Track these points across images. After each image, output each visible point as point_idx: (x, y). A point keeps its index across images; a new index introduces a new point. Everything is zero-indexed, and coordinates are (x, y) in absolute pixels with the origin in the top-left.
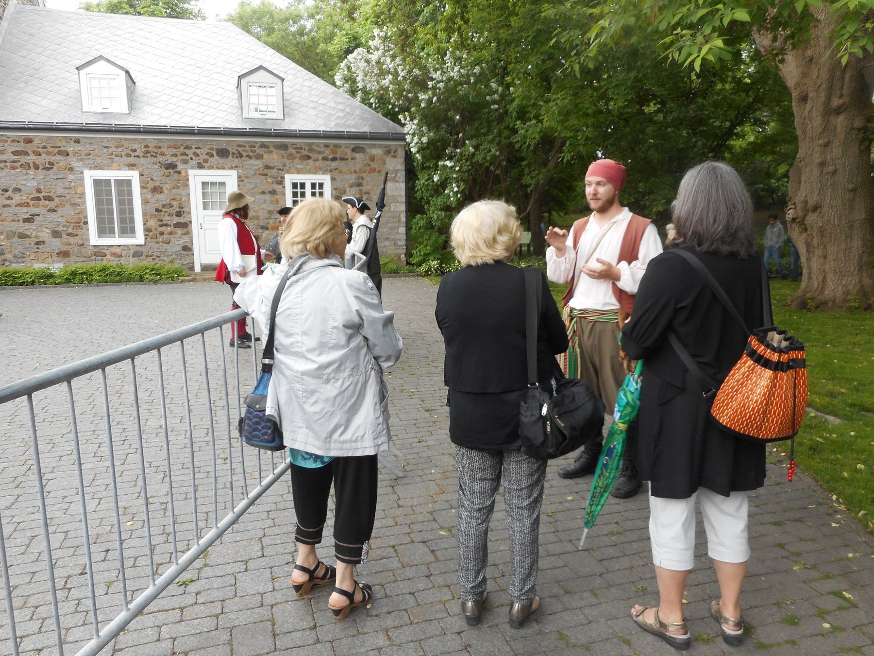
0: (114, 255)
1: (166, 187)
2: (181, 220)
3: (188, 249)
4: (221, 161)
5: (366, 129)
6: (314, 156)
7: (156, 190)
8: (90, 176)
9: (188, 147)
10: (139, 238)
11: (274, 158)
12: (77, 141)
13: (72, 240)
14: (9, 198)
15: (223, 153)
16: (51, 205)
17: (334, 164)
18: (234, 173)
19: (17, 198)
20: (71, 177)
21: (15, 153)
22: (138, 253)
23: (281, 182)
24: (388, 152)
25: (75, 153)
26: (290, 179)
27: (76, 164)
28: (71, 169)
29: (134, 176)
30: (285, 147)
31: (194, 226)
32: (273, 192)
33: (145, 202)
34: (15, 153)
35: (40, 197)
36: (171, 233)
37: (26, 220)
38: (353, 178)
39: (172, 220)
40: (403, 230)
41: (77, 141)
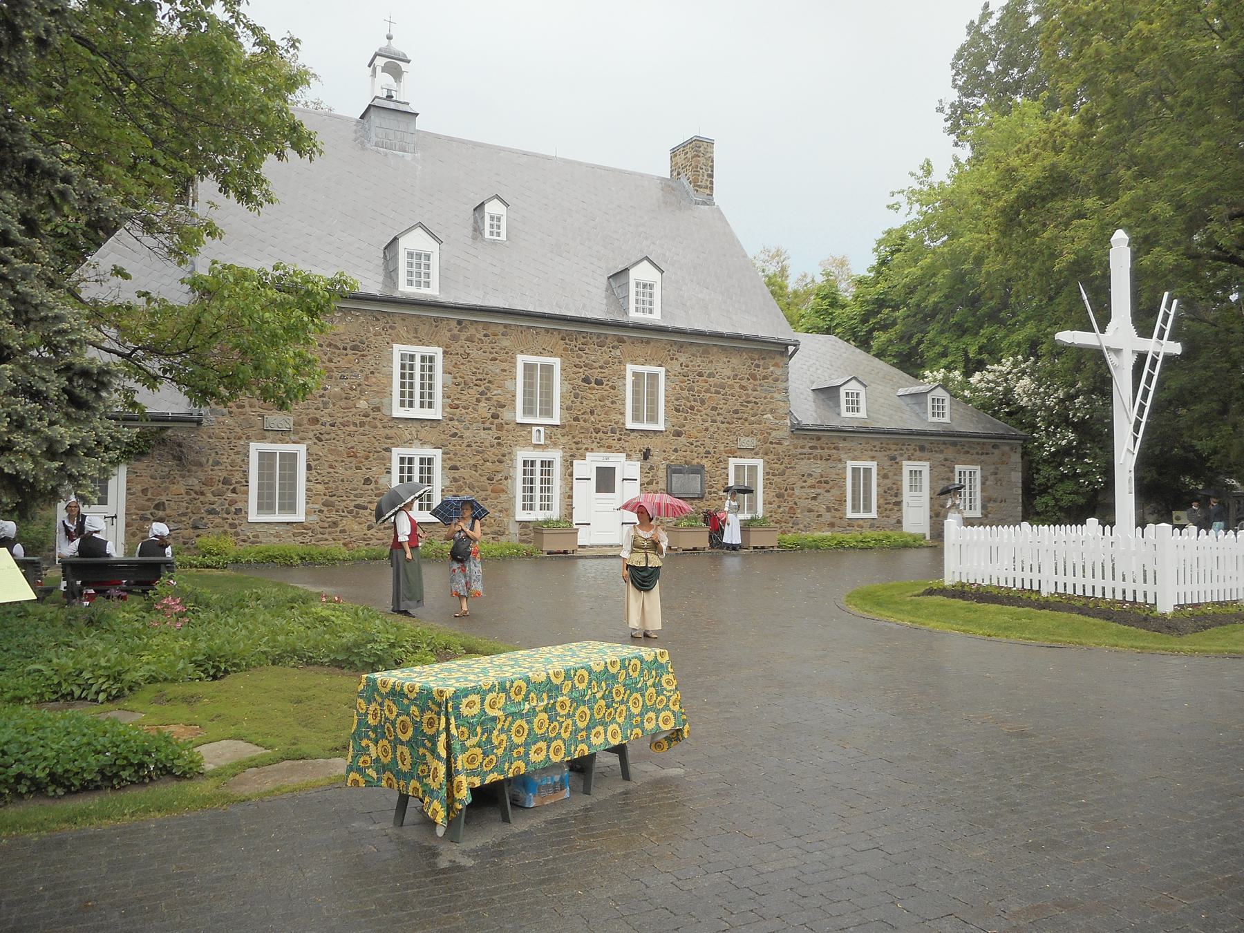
1: (890, 474)
3: (899, 522)
5: (980, 430)
7: (885, 477)
8: (851, 464)
10: (874, 515)
11: (950, 453)
13: (838, 514)
15: (922, 449)
16: (828, 487)
17: (983, 457)
18: (927, 464)
21: (811, 448)
22: (872, 524)
23: (952, 471)
24: (1012, 449)
25: (843, 448)
26: (958, 468)
27: (843, 456)
29: (873, 465)
31: (904, 504)
34: (811, 448)
35: (823, 481)
37: (814, 499)
38: (992, 469)
39: (892, 500)
40: (1020, 509)
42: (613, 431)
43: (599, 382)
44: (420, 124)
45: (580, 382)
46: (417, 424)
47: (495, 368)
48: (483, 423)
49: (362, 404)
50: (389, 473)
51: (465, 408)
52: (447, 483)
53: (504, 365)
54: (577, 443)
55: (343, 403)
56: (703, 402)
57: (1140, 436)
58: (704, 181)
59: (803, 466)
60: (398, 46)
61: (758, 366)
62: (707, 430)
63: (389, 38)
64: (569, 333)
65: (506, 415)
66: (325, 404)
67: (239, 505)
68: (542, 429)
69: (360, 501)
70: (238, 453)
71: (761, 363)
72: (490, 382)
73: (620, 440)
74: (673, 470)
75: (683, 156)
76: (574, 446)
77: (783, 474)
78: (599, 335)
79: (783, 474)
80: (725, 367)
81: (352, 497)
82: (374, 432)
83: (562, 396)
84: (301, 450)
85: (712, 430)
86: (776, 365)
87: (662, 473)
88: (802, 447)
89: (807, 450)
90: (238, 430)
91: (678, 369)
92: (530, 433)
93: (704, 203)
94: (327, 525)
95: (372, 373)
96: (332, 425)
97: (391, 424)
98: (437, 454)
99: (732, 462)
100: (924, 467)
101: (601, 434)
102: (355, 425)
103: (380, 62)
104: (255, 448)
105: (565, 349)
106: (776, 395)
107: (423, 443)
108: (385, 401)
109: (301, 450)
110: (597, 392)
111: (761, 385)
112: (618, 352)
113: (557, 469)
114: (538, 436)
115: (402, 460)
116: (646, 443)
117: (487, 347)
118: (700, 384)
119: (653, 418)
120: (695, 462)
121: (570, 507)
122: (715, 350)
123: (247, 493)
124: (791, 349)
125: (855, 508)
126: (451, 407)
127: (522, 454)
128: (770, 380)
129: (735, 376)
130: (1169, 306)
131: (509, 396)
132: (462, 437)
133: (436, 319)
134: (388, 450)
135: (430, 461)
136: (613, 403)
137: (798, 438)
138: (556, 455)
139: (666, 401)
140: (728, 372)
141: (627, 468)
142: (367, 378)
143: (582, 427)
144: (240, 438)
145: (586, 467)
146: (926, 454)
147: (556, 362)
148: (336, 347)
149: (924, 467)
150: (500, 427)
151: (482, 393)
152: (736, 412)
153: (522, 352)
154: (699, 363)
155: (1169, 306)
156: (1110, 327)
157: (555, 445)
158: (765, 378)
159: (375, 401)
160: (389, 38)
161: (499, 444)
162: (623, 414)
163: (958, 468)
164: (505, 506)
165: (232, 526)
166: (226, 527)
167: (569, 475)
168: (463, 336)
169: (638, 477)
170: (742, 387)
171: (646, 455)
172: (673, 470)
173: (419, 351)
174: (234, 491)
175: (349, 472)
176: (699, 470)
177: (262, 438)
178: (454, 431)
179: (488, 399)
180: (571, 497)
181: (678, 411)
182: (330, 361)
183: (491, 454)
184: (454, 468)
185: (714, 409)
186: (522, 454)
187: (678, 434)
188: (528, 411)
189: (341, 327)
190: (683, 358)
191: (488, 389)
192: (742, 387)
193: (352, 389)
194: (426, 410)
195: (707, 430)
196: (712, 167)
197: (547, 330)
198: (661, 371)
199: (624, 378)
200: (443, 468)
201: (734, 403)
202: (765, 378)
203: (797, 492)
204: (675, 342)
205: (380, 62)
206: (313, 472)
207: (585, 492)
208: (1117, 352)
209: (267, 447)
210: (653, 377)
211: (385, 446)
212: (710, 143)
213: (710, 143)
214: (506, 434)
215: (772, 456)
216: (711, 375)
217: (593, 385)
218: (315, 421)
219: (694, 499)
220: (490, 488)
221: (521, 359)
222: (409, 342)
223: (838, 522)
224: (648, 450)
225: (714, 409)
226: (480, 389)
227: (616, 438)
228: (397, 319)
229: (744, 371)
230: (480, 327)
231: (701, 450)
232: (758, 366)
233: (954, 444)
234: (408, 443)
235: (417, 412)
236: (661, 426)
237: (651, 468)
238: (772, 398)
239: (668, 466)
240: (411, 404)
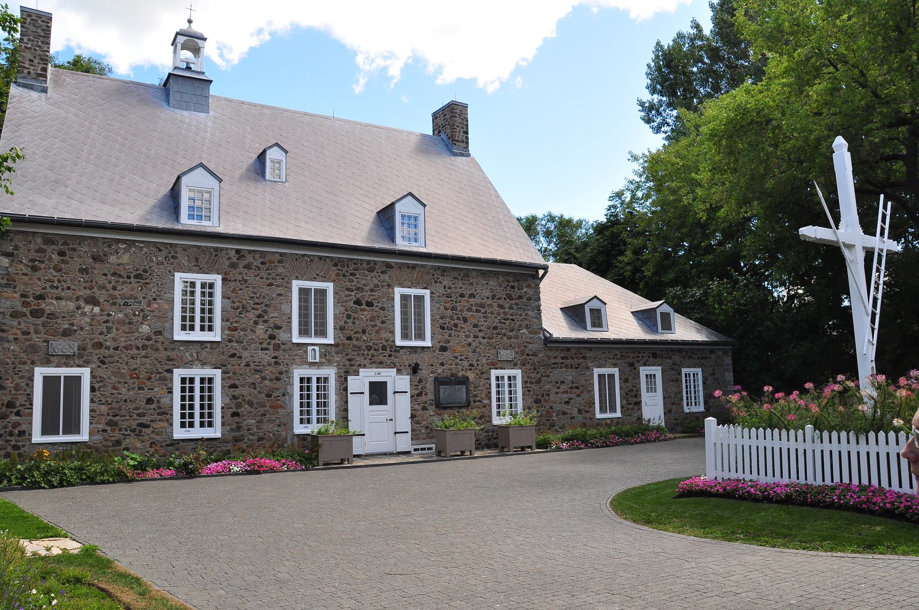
0: (607, 424)
1: (630, 378)
2: (637, 400)
4: (655, 360)
6: (694, 356)
8: (597, 371)
9: (640, 353)
10: (618, 414)
11: (677, 358)
12: (591, 349)
13: (588, 415)
14: (559, 388)
15: (655, 356)
19: (563, 388)
20: (588, 373)
21: (562, 358)
23: (680, 374)
24: (724, 353)
26: (684, 371)
27: (590, 365)
28: (588, 368)
29: (615, 371)
30: (680, 351)
31: (643, 404)
32: (677, 380)
33: (621, 389)
34: (562, 358)
36: (633, 409)
37: (567, 403)
39: (633, 400)
41: (591, 349)
42: (384, 348)
43: (369, 304)
44: (213, 90)
45: (352, 304)
46: (198, 347)
47: (273, 292)
48: (261, 343)
50: (171, 392)
51: (243, 330)
52: (227, 401)
53: (280, 290)
54: (350, 360)
55: (126, 328)
56: (465, 320)
57: (877, 326)
58: (460, 136)
59: (556, 375)
60: (196, 28)
61: (513, 287)
62: (470, 345)
63: (190, 22)
64: (341, 260)
65: (282, 336)
66: (109, 330)
67: (23, 427)
68: (317, 348)
69: (144, 420)
70: (22, 377)
71: (516, 284)
72: (266, 305)
73: (390, 356)
74: (439, 382)
75: (442, 118)
76: (347, 363)
77: (539, 381)
78: (369, 262)
79: (539, 381)
80: (484, 290)
81: (135, 416)
82: (157, 355)
83: (335, 317)
84: (85, 374)
85: (474, 344)
86: (529, 286)
87: (430, 386)
88: (555, 358)
89: (559, 360)
90: (22, 355)
91: (442, 290)
92: (306, 352)
93: (462, 155)
94: (110, 444)
95: (155, 299)
96: (116, 349)
97: (172, 346)
98: (217, 374)
99: (494, 373)
100: (657, 371)
101: (372, 351)
102: (138, 348)
103: (181, 39)
104: (40, 373)
105: (338, 275)
106: (530, 313)
107: (203, 364)
108: (167, 325)
109: (85, 374)
110: (367, 314)
111: (516, 304)
112: (386, 277)
113: (332, 384)
114: (313, 355)
115: (183, 380)
117: (264, 274)
118: (462, 304)
119: (420, 336)
120: (460, 374)
121: (345, 419)
122: (474, 273)
123: (31, 415)
124: (541, 272)
125: (603, 410)
126: (230, 329)
127: (298, 373)
128: (524, 300)
129: (493, 297)
130: (885, 207)
131: (285, 318)
132: (240, 357)
133: (216, 249)
134: (170, 371)
135: (210, 380)
136: (383, 322)
137: (551, 349)
138: (330, 373)
139: (432, 320)
140: (487, 293)
141: (398, 382)
142: (149, 305)
143: (354, 346)
144: (25, 363)
145: (360, 382)
146: (658, 360)
147: (329, 287)
148: (120, 276)
149: (657, 371)
150: (277, 347)
151: (260, 316)
152: (495, 328)
153: (297, 278)
154: (461, 286)
155: (885, 207)
156: (842, 224)
157: (330, 363)
158: (520, 297)
159: (158, 326)
160: (190, 22)
161: (276, 363)
162: (393, 332)
163: (684, 371)
164: (284, 421)
165: (16, 447)
166: (9, 449)
167: (343, 390)
168: (242, 264)
169: (408, 389)
170: (500, 306)
171: (415, 369)
172: (439, 382)
173: (199, 278)
174: (18, 414)
175: (132, 393)
176: (464, 381)
177: (47, 362)
178: (232, 351)
179: (265, 321)
180: (346, 410)
181: (442, 328)
182: (114, 288)
183: (269, 372)
184: (233, 386)
185: (476, 326)
186: (298, 373)
187: (444, 349)
188: (304, 331)
189: (124, 259)
190: (446, 282)
191: (265, 312)
192: (500, 306)
193: (135, 315)
194: (207, 333)
195: (470, 345)
196: (467, 125)
197: (320, 258)
198: (427, 293)
199: (393, 299)
200: (223, 387)
201: (493, 321)
202: (520, 297)
203: (552, 397)
204: (439, 268)
205: (181, 39)
206: (97, 393)
207: (359, 405)
208: (850, 247)
210: (420, 299)
211: (167, 367)
212: (465, 107)
213: (465, 107)
214: (285, 353)
215: (528, 366)
216: (472, 296)
217: (364, 306)
218: (99, 345)
219: (460, 407)
220: (268, 405)
221: (296, 285)
222: (190, 271)
223: (588, 422)
224: (417, 365)
225: (476, 326)
226: (259, 312)
227: (387, 354)
228: (178, 249)
229: (501, 292)
230: (257, 256)
231: (466, 363)
232: (513, 287)
233: (680, 351)
234: (188, 364)
235: (197, 335)
236: (428, 343)
237: (420, 381)
238: (527, 315)
239: (436, 379)
240: (192, 328)
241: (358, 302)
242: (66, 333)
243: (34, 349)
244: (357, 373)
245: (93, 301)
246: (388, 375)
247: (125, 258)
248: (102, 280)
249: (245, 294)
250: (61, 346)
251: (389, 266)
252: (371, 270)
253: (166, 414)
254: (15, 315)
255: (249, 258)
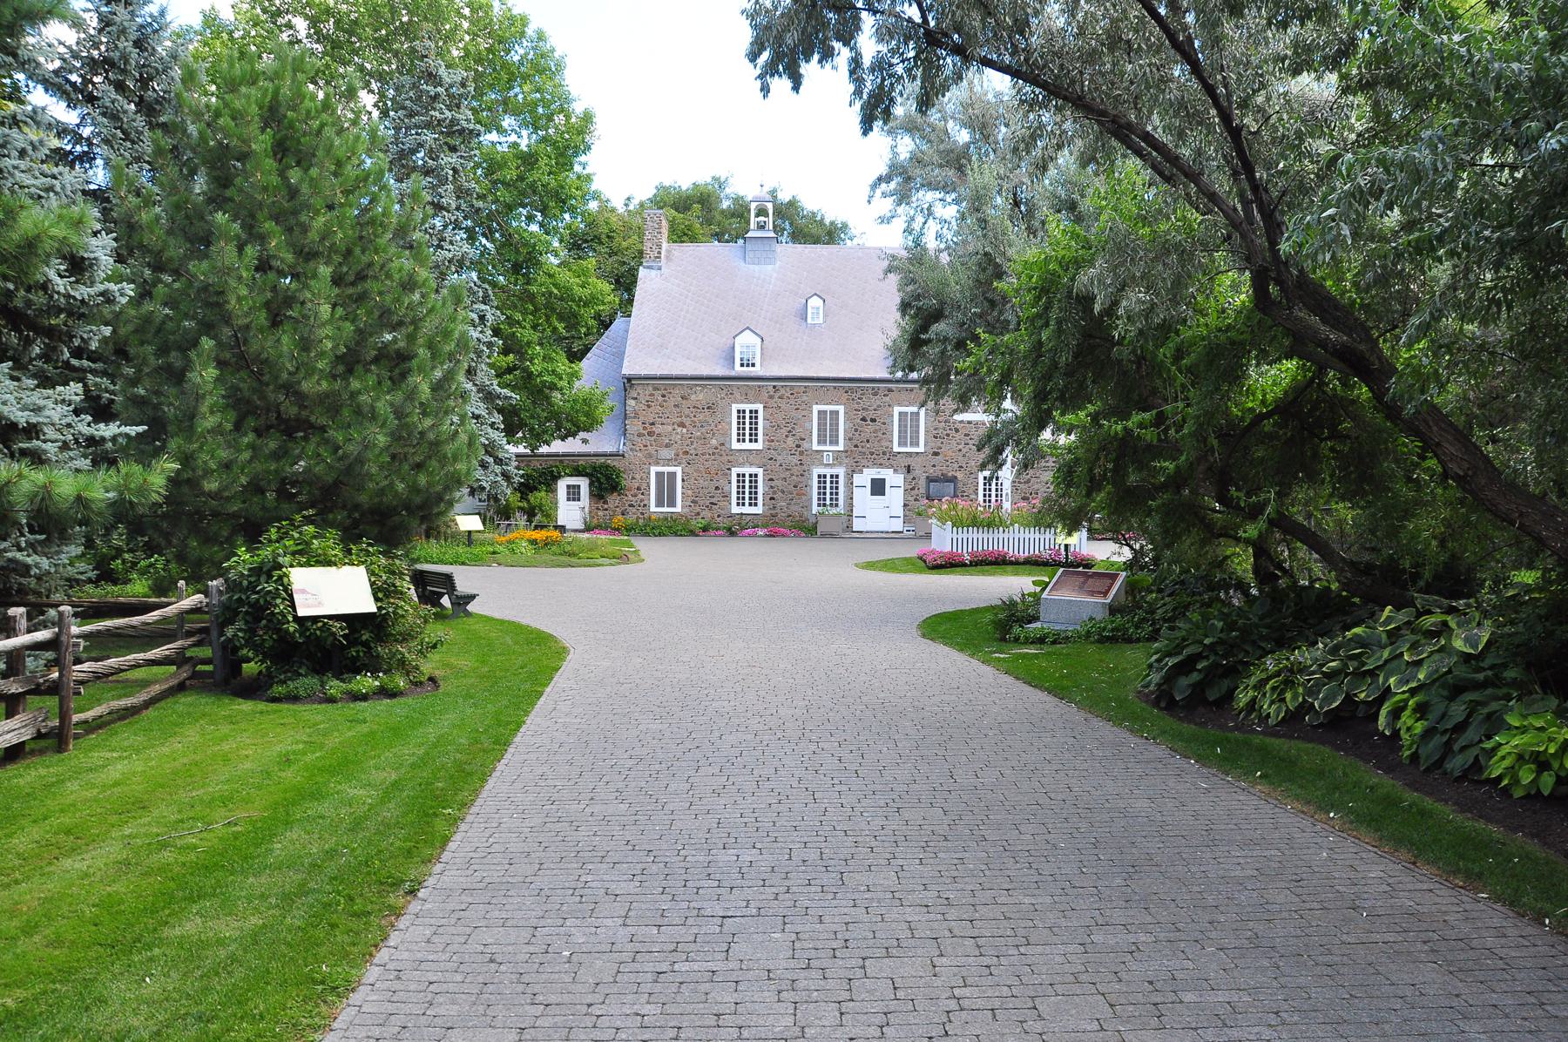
43: (873, 420)
47: (799, 415)
49: (714, 442)
65: (805, 445)
74: (930, 480)
77: (1028, 481)
84: (679, 470)
87: (922, 482)
98: (760, 471)
104: (654, 470)
109: (679, 470)
116: (909, 461)
127: (816, 471)
145: (864, 478)
147: (841, 409)
157: (840, 464)
159: (722, 440)
167: (849, 483)
171: (909, 469)
172: (930, 480)
173: (748, 407)
176: (953, 480)
177: (657, 464)
183: (796, 470)
187: (936, 454)
189: (700, 396)
207: (862, 497)
209: (660, 469)
218: (686, 453)
221: (816, 408)
227: (886, 458)
235: (747, 445)
236: (921, 449)
241: (864, 419)
242: (667, 446)
243: (650, 456)
244: (861, 472)
245: (682, 425)
246: (888, 475)
247: (701, 397)
248: (687, 411)
249: (780, 416)
250: (666, 453)
251: (890, 390)
252: (875, 394)
253: (727, 496)
254: (639, 435)
255: (783, 391)
